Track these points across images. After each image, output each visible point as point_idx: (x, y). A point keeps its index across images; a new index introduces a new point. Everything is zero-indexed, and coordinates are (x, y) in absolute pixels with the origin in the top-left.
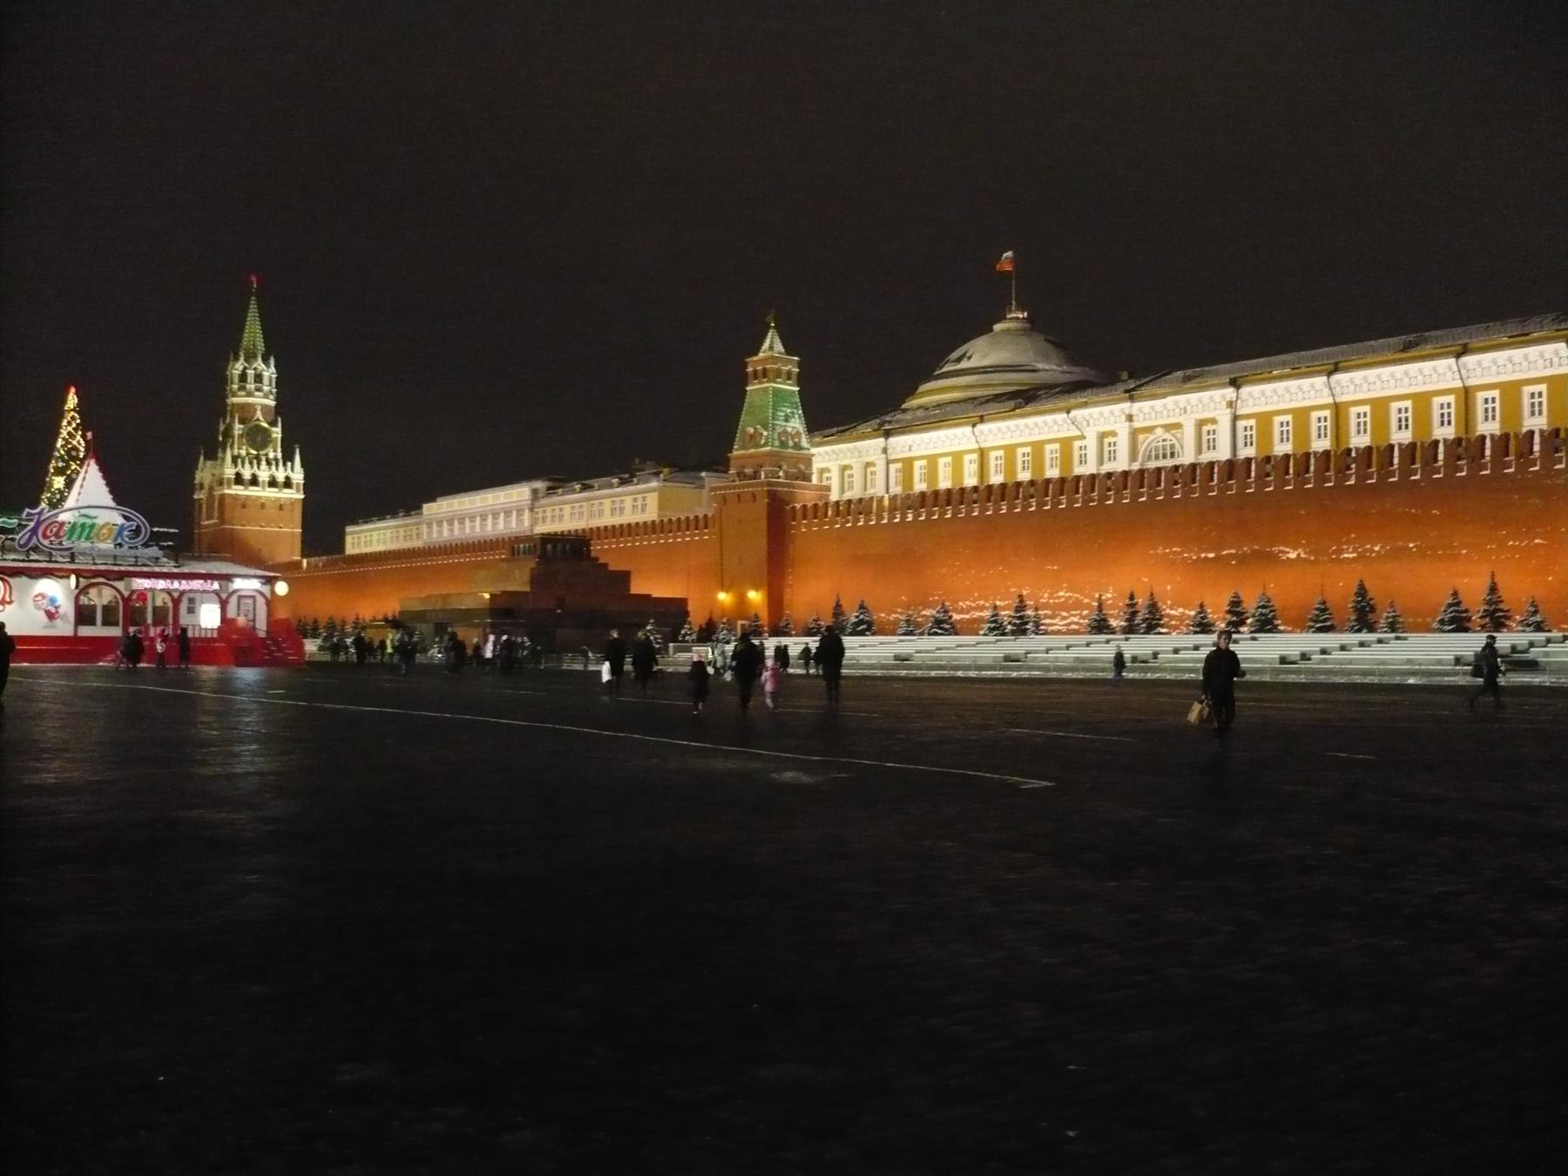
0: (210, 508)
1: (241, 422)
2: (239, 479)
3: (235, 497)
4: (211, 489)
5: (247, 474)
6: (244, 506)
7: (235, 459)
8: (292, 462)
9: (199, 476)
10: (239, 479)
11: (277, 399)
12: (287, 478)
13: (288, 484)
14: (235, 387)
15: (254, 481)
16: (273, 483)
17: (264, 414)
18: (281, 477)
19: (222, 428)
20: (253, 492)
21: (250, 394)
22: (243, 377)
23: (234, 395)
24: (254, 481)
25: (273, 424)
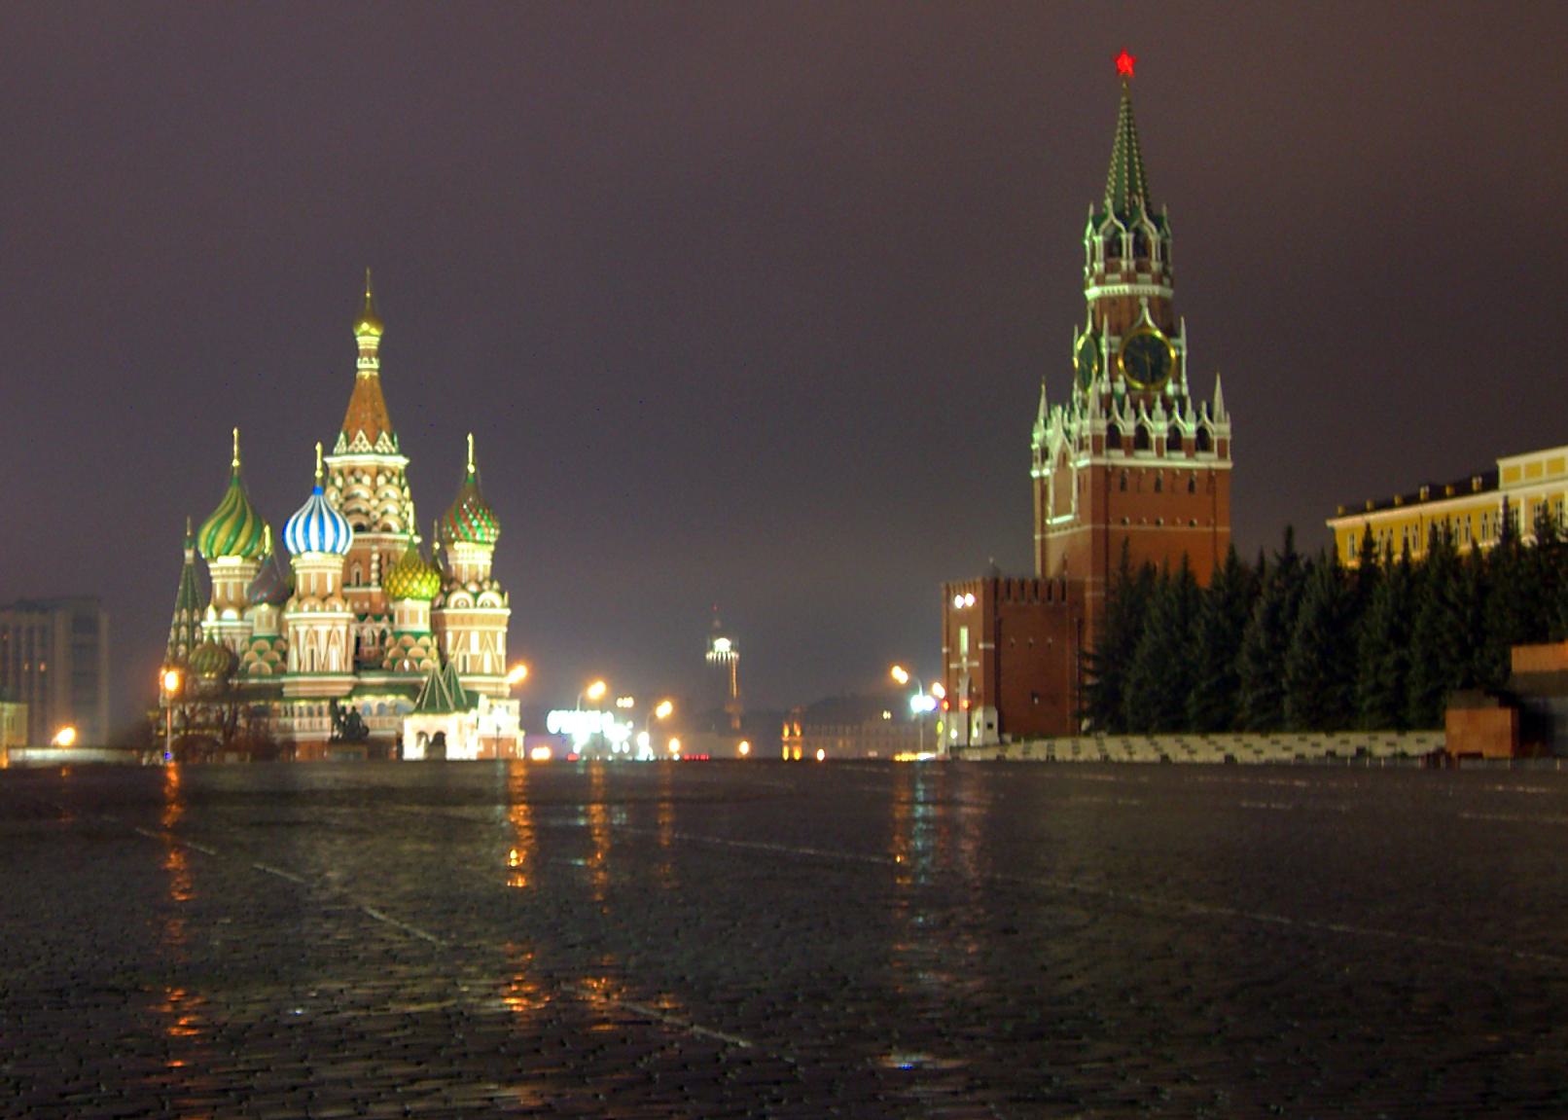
0: (1063, 493)
2: (1114, 438)
4: (1064, 458)
5: (1127, 427)
6: (1123, 486)
7: (1106, 402)
9: (1037, 436)
12: (1202, 432)
13: (1203, 441)
14: (1099, 266)
15: (1142, 440)
16: (1175, 441)
18: (1189, 428)
19: (1079, 345)
20: (1146, 460)
21: (1129, 278)
24: (1142, 440)
25: (1171, 332)
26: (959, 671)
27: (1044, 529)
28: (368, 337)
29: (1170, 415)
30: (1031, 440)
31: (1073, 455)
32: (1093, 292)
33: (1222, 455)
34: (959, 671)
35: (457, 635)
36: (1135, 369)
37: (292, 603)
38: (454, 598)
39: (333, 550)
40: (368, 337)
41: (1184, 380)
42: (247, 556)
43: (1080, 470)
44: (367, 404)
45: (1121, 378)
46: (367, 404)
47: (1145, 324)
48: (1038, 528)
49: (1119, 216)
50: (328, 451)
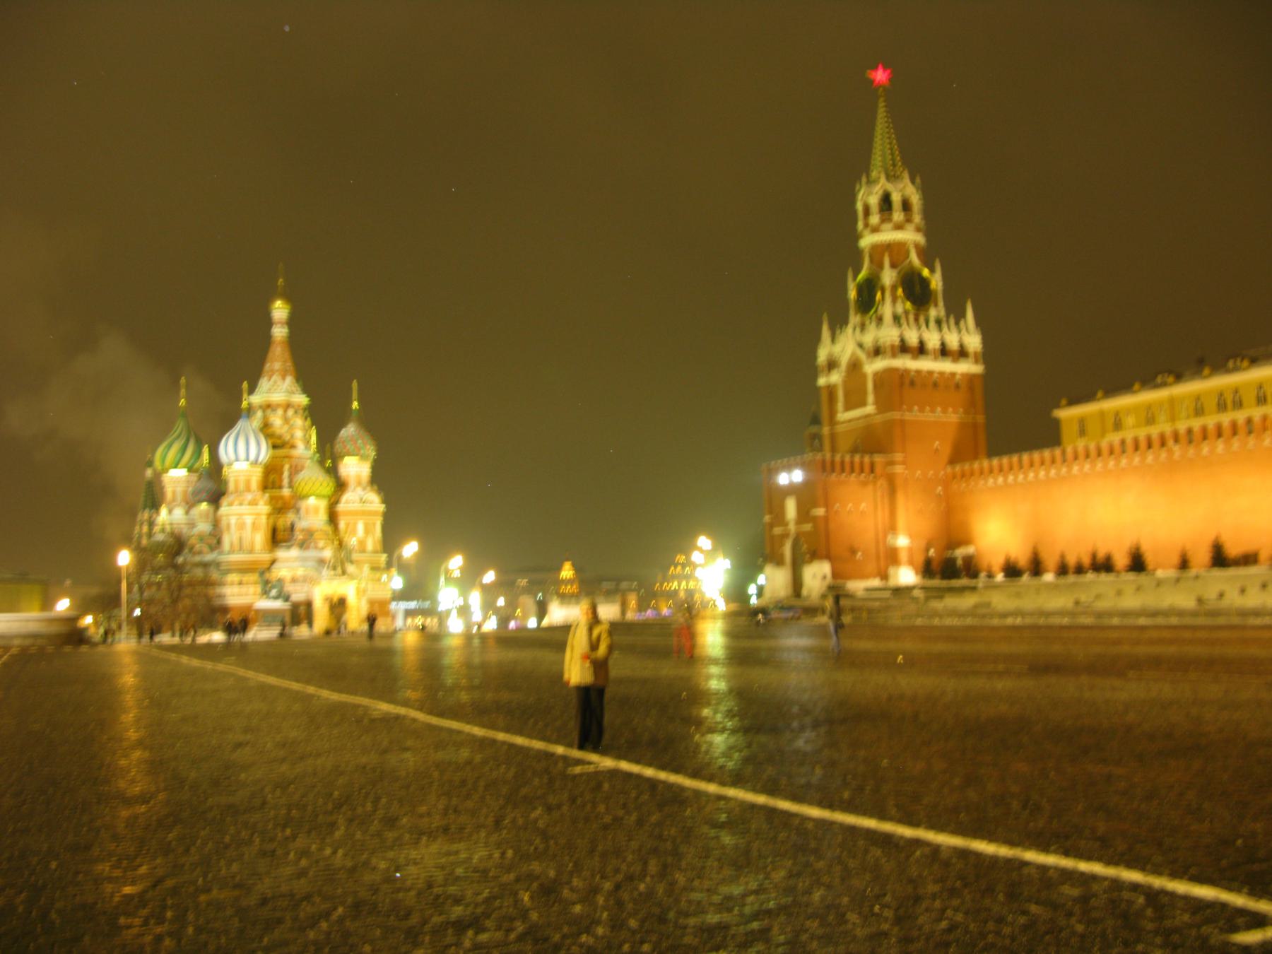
1: (893, 266)
4: (855, 366)
7: (896, 319)
13: (962, 353)
15: (921, 350)
16: (944, 352)
18: (953, 340)
21: (899, 227)
28: (280, 310)
30: (815, 357)
33: (976, 362)
35: (348, 525)
37: (224, 501)
38: (345, 497)
39: (256, 462)
40: (280, 310)
41: (941, 303)
42: (190, 470)
44: (278, 358)
46: (278, 358)
50: (252, 391)
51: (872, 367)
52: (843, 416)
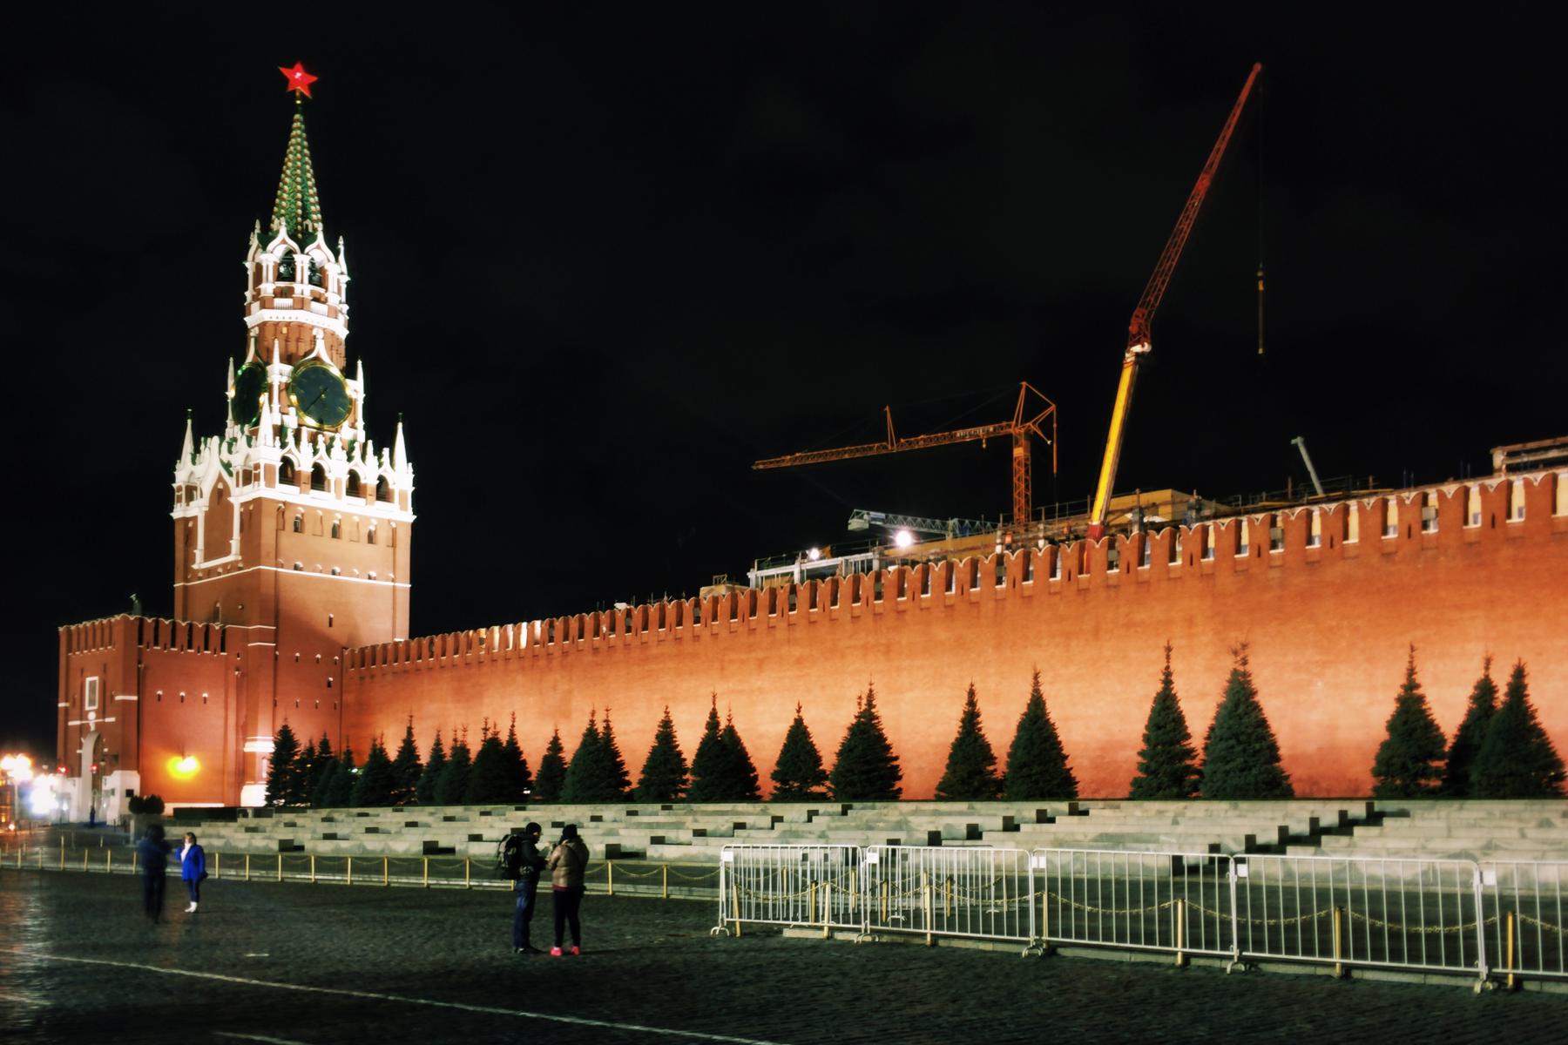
1: (287, 359)
2: (287, 473)
3: (282, 509)
4: (220, 495)
5: (304, 464)
6: (298, 527)
7: (280, 431)
8: (391, 445)
10: (287, 473)
11: (351, 325)
16: (354, 486)
17: (330, 348)
21: (301, 304)
22: (287, 270)
23: (265, 304)
24: (318, 478)
25: (350, 372)
26: (83, 730)
27: (188, 572)
29: (350, 459)
31: (234, 490)
32: (255, 317)
34: (83, 730)
36: (305, 407)
43: (243, 505)
45: (292, 411)
47: (317, 358)
48: (179, 573)
49: (293, 236)
51: (240, 496)
52: (200, 564)
